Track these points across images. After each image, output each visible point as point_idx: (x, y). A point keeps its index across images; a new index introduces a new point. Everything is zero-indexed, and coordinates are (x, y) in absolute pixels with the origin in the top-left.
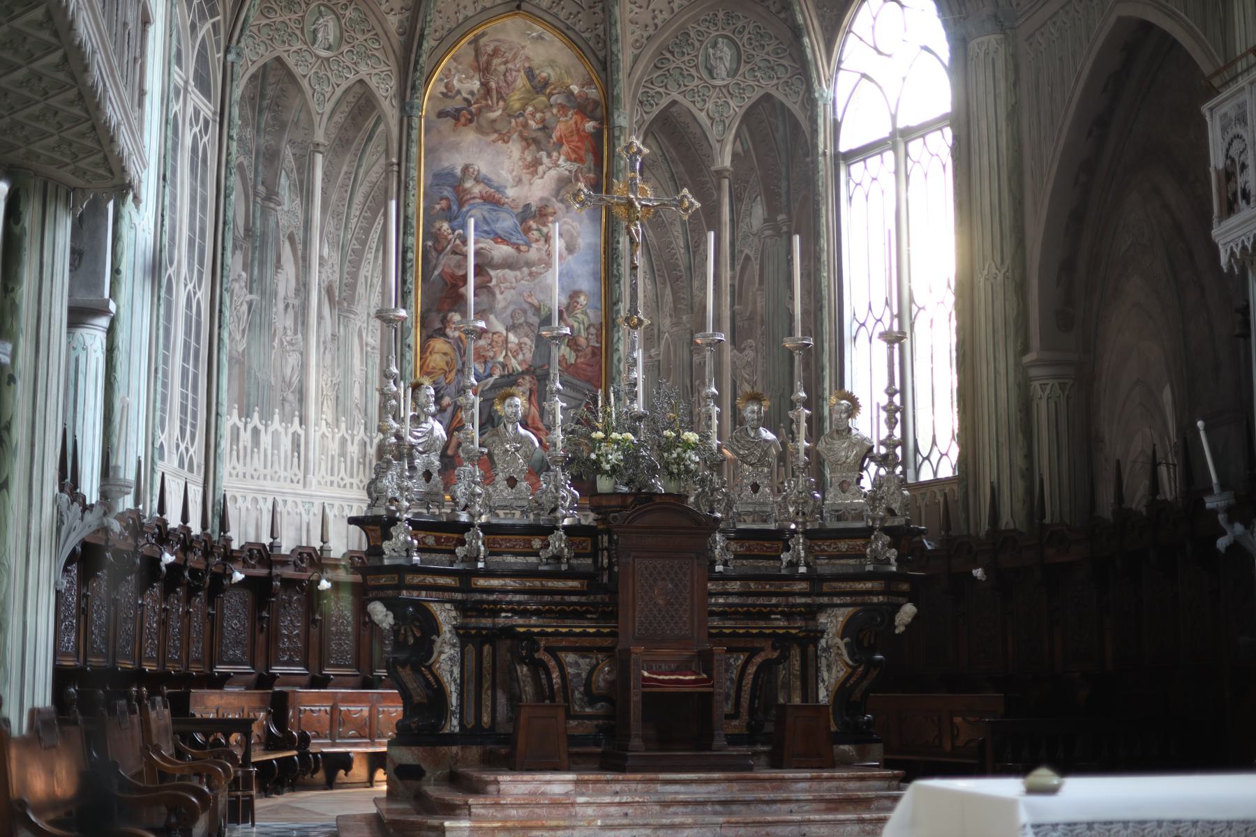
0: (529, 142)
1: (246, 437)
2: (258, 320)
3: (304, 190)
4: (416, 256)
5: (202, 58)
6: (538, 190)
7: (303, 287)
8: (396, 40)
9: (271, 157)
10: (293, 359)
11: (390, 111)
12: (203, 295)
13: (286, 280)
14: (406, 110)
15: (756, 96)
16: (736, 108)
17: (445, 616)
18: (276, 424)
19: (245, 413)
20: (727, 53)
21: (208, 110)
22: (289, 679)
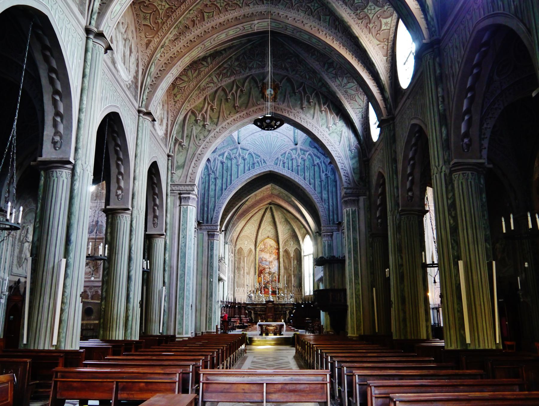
0: (270, 253)
1: (238, 290)
2: (239, 277)
3: (244, 262)
4: (257, 268)
5: (232, 250)
6: (271, 259)
7: (244, 273)
8: (254, 242)
9: (240, 258)
10: (243, 281)
11: (254, 251)
12: (233, 276)
13: (242, 272)
14: (255, 250)
15: (295, 248)
16: (293, 249)
17: (252, 312)
18: (241, 289)
19: (238, 288)
20: (292, 242)
21: (233, 255)
22: (243, 317)
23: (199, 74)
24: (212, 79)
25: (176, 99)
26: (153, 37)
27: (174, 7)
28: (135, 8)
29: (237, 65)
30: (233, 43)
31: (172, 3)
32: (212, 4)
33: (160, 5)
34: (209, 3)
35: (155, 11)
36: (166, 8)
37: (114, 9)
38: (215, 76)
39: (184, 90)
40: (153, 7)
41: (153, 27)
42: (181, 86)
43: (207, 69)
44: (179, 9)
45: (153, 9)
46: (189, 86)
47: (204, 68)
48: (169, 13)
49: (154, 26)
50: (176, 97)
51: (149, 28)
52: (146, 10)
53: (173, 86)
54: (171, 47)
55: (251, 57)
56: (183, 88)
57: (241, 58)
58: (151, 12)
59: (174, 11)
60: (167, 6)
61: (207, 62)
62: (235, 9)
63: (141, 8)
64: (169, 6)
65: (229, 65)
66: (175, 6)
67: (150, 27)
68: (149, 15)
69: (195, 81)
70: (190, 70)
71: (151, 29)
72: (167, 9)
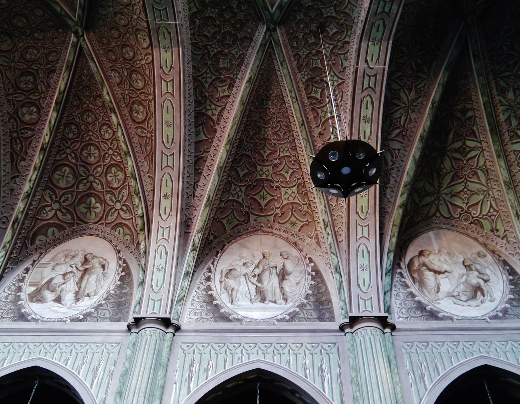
23: (486, 172)
24: (514, 151)
25: (501, 233)
26: (316, 229)
27: (300, 181)
28: (276, 229)
29: (515, 94)
30: (434, 99)
31: (295, 181)
32: (323, 125)
33: (288, 197)
34: (320, 129)
35: (293, 208)
36: (296, 192)
37: (154, 281)
38: (512, 144)
39: (495, 210)
40: (287, 207)
41: (307, 221)
42: (485, 212)
43: (486, 154)
44: (305, 176)
45: (289, 208)
46: (495, 200)
47: (481, 157)
48: (303, 191)
49: (306, 219)
50: (497, 230)
51: (306, 226)
52: (286, 217)
53: (476, 224)
54: (341, 213)
55: (511, 62)
56: (492, 210)
57: (502, 83)
58: (291, 213)
59: (304, 183)
60: (295, 189)
61: (472, 149)
62: (343, 92)
63: (281, 222)
64: (296, 187)
65: (507, 110)
66: (300, 179)
67: (305, 224)
68: (293, 217)
69: (493, 183)
70: (468, 183)
71: (308, 225)
72: (298, 191)
